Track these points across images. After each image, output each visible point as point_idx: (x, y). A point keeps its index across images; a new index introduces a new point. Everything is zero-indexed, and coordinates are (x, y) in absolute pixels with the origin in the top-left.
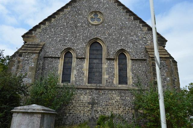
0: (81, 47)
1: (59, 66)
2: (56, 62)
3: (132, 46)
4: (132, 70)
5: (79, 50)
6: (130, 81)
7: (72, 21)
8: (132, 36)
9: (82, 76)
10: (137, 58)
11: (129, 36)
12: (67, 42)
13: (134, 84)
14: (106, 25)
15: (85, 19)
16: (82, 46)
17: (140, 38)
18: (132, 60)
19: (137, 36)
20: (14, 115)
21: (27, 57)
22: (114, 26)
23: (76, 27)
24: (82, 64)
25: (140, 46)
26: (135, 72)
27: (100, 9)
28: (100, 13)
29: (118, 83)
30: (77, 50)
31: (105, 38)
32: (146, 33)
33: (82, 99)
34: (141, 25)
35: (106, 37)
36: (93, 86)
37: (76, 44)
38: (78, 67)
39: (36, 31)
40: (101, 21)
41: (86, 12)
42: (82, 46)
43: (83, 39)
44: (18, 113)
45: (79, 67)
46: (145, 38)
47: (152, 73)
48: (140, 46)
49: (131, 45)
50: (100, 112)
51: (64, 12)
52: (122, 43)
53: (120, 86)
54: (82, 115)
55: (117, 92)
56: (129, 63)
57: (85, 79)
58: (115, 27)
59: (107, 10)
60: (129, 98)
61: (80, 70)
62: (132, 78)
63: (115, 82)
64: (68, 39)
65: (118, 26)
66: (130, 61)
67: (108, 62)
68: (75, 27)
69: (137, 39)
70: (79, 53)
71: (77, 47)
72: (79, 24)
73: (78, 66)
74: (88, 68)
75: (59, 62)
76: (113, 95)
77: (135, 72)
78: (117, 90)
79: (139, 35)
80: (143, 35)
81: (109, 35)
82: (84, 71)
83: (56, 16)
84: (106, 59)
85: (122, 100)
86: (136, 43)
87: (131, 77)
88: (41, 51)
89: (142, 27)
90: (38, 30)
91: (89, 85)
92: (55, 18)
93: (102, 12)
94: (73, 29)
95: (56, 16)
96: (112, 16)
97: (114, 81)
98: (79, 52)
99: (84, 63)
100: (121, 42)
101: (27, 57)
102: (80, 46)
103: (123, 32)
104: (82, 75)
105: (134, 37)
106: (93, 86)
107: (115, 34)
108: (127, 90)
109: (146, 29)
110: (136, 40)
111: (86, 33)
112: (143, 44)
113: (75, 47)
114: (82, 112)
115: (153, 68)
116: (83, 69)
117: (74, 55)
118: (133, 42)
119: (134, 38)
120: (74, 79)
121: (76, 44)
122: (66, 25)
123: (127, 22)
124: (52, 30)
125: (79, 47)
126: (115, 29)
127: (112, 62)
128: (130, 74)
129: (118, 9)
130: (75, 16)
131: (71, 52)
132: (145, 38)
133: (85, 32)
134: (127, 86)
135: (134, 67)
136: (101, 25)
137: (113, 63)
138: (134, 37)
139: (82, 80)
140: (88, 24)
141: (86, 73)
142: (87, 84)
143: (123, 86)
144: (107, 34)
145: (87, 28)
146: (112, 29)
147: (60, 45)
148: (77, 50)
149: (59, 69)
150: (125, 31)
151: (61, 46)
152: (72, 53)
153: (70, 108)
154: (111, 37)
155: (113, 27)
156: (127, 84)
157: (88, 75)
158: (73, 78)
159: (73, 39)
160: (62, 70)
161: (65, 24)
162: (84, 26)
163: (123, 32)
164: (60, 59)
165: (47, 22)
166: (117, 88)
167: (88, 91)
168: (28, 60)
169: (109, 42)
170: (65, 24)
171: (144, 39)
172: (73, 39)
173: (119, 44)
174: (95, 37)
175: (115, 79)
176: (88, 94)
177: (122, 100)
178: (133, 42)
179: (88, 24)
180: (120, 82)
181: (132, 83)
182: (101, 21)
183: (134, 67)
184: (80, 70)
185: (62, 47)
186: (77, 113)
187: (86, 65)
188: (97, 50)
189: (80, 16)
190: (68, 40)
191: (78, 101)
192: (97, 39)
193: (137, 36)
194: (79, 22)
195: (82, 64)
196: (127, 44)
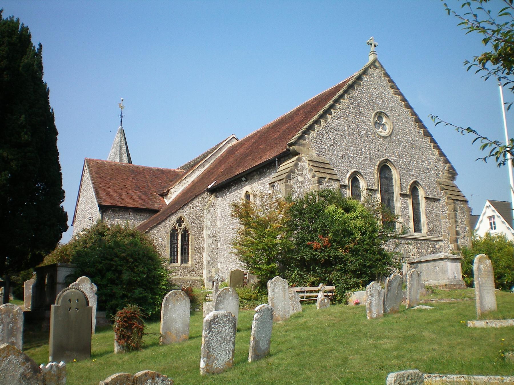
4: (427, 213)
6: (424, 228)
23: (360, 136)
28: (387, 116)
34: (432, 145)
39: (309, 135)
40: (387, 131)
47: (454, 220)
48: (433, 179)
53: (416, 234)
69: (429, 167)
79: (431, 161)
81: (400, 157)
84: (401, 194)
87: (426, 223)
90: (312, 134)
92: (331, 114)
93: (388, 114)
94: (355, 139)
100: (412, 169)
102: (368, 170)
109: (437, 153)
124: (330, 136)
130: (356, 116)
140: (374, 133)
143: (417, 235)
150: (416, 153)
164: (347, 188)
165: (322, 120)
171: (436, 168)
177: (419, 252)
178: (425, 170)
182: (387, 131)
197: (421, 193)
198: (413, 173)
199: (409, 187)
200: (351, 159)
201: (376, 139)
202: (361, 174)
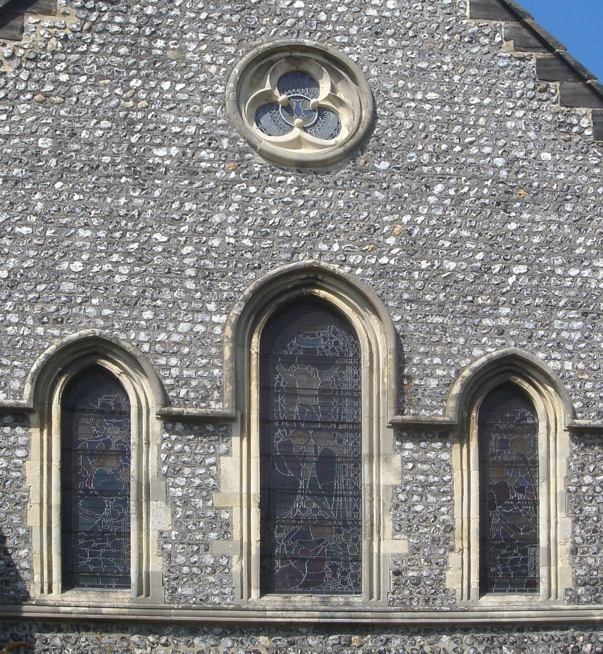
1: (32, 470)
5: (173, 361)
7: (105, 124)
9: (218, 547)
11: (559, 261)
12: (70, 295)
14: (384, 165)
15: (206, 109)
16: (200, 328)
22: (443, 178)
23: (142, 173)
24: (211, 460)
27: (336, 33)
30: (162, 361)
31: (383, 272)
35: (384, 260)
37: (148, 315)
38: (181, 481)
40: (344, 134)
41: (215, 48)
42: (200, 328)
43: (203, 274)
45: (189, 484)
51: (26, 42)
52: (505, 310)
58: (459, 187)
59: (391, 42)
64: (77, 266)
65: (478, 180)
67: (409, 445)
70: (177, 379)
71: (162, 336)
72: (162, 152)
73: (177, 473)
75: (27, 446)
81: (413, 248)
82: (229, 509)
84: (394, 425)
96: (432, 95)
98: (175, 372)
99: (228, 453)
102: (184, 327)
103: (513, 226)
104: (213, 535)
107: (454, 240)
111: (222, 225)
113: (143, 336)
116: (216, 500)
117: (140, 392)
120: (157, 565)
121: (148, 315)
122: (54, 153)
125: (176, 338)
126: (458, 200)
127: (438, 445)
129: (473, 39)
131: (115, 370)
133: (217, 219)
137: (444, 456)
144: (391, 241)
145: (228, 185)
146: (432, 199)
148: (162, 361)
149: (34, 498)
150: (530, 222)
151: (30, 322)
152: (124, 380)
154: (424, 264)
155: (439, 188)
159: (124, 270)
161: (45, 143)
162: (207, 171)
163: (513, 226)
169: (409, 301)
170: (45, 143)
172: (124, 270)
173: (487, 322)
174: (303, 260)
179: (242, 152)
182: (344, 134)
184: (200, 503)
185: (40, 330)
187: (237, 467)
188: (323, 362)
189: (166, 85)
190: (83, 279)
192: (315, 275)
195: (211, 460)
197: (551, 412)
198: (505, 321)
199: (456, 389)
200: (67, 287)
202: (123, 350)
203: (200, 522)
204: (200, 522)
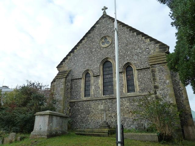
0: (96, 67)
1: (82, 84)
2: (79, 82)
3: (136, 58)
4: (138, 79)
6: (137, 89)
8: (136, 50)
10: (142, 68)
12: (86, 66)
13: (140, 91)
17: (143, 50)
18: (138, 70)
19: (141, 49)
20: (36, 117)
21: (59, 82)
23: (91, 52)
25: (144, 57)
26: (140, 80)
29: (127, 92)
32: (148, 44)
33: (99, 108)
36: (107, 96)
38: (95, 83)
41: (98, 39)
44: (38, 115)
46: (148, 48)
47: (152, 79)
48: (144, 57)
49: (135, 57)
50: (114, 117)
53: (129, 94)
54: (100, 120)
55: (126, 99)
56: (135, 73)
57: (101, 92)
60: (137, 103)
61: (97, 85)
62: (139, 86)
63: (124, 92)
66: (136, 71)
68: (91, 52)
69: (141, 51)
73: (95, 82)
74: (102, 83)
76: (123, 102)
77: (140, 80)
78: (126, 97)
79: (143, 47)
80: (146, 46)
83: (77, 47)
85: (131, 105)
86: (140, 55)
87: (138, 85)
88: (68, 76)
89: (144, 40)
90: (66, 61)
91: (104, 96)
92: (76, 49)
95: (77, 47)
97: (123, 90)
100: (127, 57)
101: (59, 82)
105: (138, 50)
106: (107, 96)
107: (121, 51)
108: (135, 96)
110: (140, 52)
112: (147, 54)
114: (100, 118)
115: (153, 74)
117: (91, 74)
118: (137, 55)
119: (139, 51)
120: (93, 93)
123: (131, 39)
126: (122, 47)
128: (136, 83)
129: (122, 29)
130: (90, 44)
132: (148, 48)
134: (135, 93)
135: (140, 76)
136: (110, 46)
138: (138, 50)
139: (99, 93)
141: (101, 87)
142: (102, 95)
143: (131, 94)
145: (99, 51)
147: (82, 69)
149: (82, 87)
153: (92, 116)
156: (128, 92)
157: (102, 88)
158: (92, 92)
160: (84, 87)
164: (82, 79)
166: (126, 96)
167: (103, 101)
168: (59, 84)
171: (147, 50)
174: (106, 57)
175: (124, 88)
176: (104, 104)
177: (131, 105)
178: (137, 55)
180: (129, 91)
181: (138, 90)
183: (140, 76)
186: (97, 119)
187: (100, 81)
188: (109, 67)
190: (87, 64)
191: (97, 110)
192: (107, 58)
193: (141, 49)
194: (93, 48)
196: (133, 58)
201: (101, 50)
203: (97, 87)
204: (97, 87)
